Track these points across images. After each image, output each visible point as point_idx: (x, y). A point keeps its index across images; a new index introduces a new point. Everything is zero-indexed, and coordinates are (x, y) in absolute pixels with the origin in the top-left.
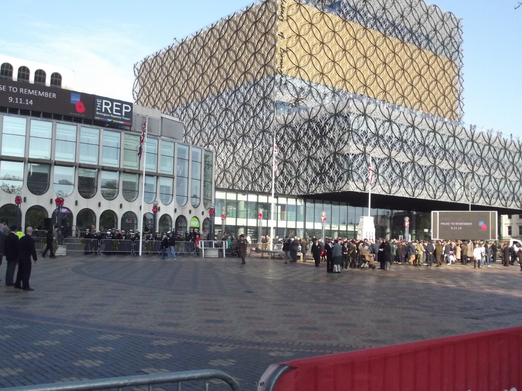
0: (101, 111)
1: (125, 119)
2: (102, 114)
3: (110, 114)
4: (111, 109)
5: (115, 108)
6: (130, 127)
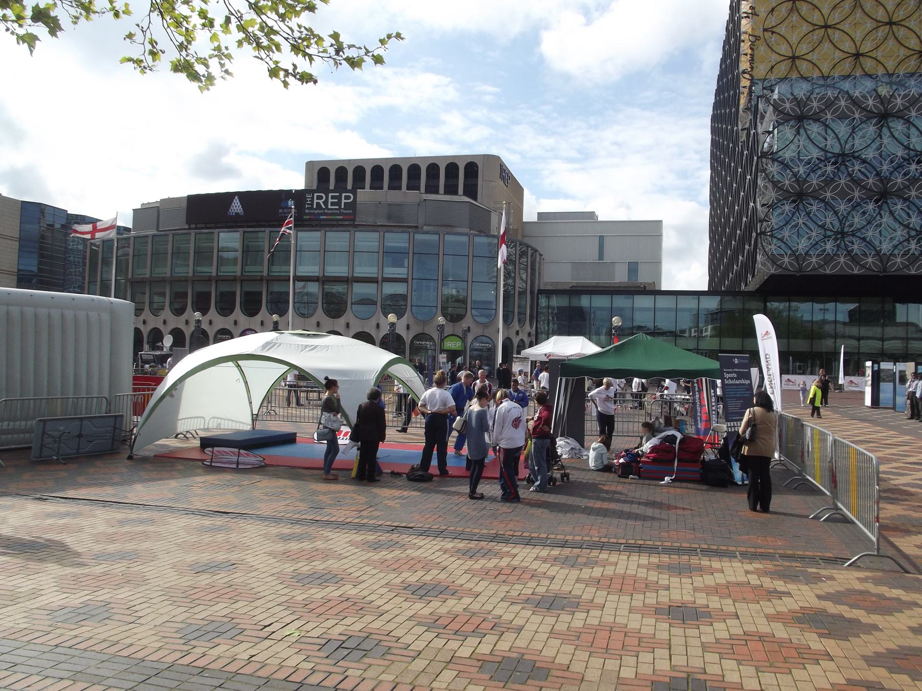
0: (312, 208)
1: (345, 212)
2: (313, 211)
3: (324, 209)
4: (326, 203)
5: (330, 200)
6: (354, 220)
